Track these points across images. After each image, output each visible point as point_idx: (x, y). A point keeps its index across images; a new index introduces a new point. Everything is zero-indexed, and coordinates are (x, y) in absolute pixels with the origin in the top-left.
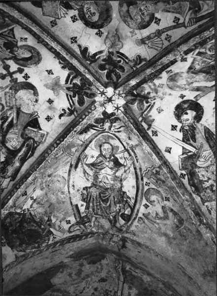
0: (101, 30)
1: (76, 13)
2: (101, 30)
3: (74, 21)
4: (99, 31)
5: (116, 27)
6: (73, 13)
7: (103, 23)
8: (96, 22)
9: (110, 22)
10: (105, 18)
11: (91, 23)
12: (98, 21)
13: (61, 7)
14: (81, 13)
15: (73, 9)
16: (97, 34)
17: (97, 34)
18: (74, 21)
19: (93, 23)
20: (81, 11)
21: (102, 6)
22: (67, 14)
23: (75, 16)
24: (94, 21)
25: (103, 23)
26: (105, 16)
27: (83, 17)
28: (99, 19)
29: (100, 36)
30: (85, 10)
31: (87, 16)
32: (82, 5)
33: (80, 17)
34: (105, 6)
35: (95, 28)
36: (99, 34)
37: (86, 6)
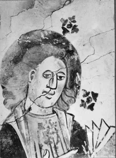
0: (60, 32)
1: (75, 108)
2: (60, 32)
3: (95, 96)
4: (65, 31)
5: (26, 12)
6: (84, 117)
7: (45, 41)
8: (56, 56)
9: (28, 34)
10: (33, 49)
11: (68, 61)
12: (52, 55)
13: (90, 148)
14: (66, 99)
15: (73, 120)
16: (75, 29)
17: (75, 29)
18: (95, 96)
19: (63, 59)
20: (61, 105)
21: (20, 77)
22: (93, 123)
23: (83, 104)
24: (58, 60)
25: (45, 41)
26: (30, 52)
27: (73, 84)
28: (47, 56)
29: (73, 19)
30: (55, 98)
31: (62, 83)
32: (54, 112)
33: (77, 93)
34: (16, 72)
35: (68, 43)
36: (71, 26)
37: (48, 103)
